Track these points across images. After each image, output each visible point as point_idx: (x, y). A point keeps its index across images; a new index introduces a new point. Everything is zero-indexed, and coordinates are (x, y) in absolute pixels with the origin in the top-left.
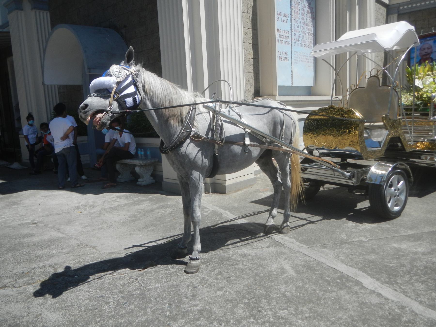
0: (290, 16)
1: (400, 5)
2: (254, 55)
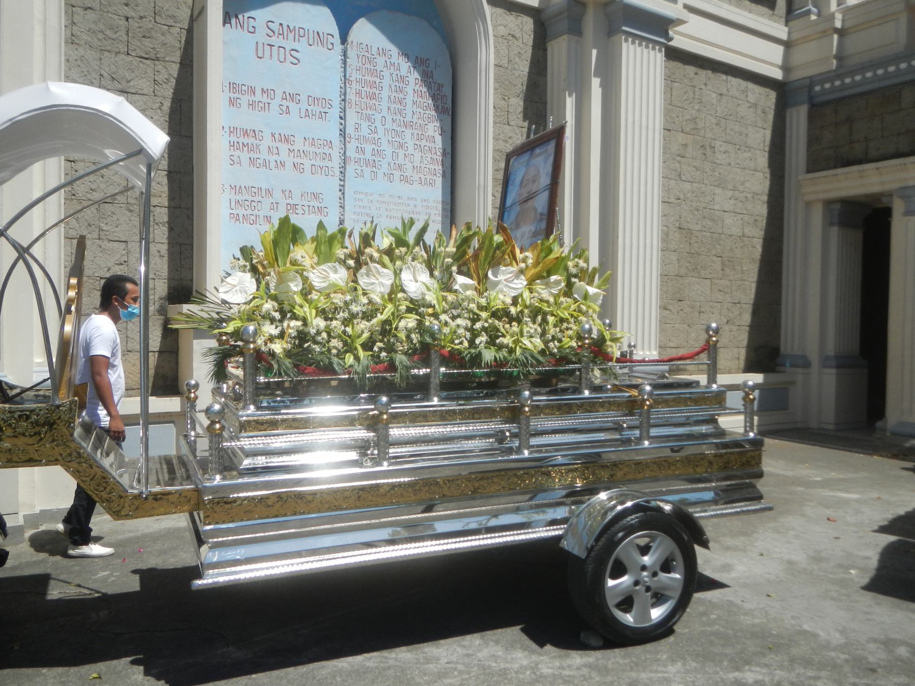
1: (812, 81)
2: (171, 198)
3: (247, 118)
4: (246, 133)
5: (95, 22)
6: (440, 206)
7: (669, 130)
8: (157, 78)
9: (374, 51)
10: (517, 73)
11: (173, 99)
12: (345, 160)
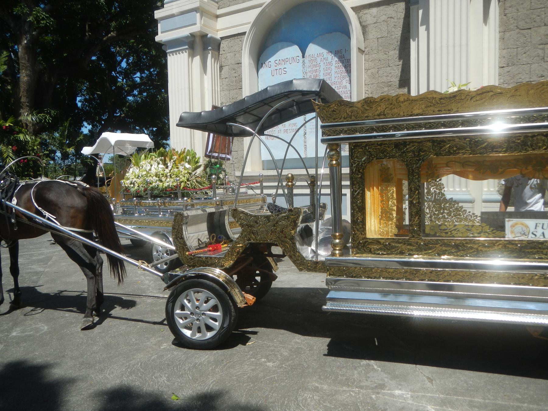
5: (228, 82)
7: (530, 28)
9: (316, 56)
10: (393, 37)
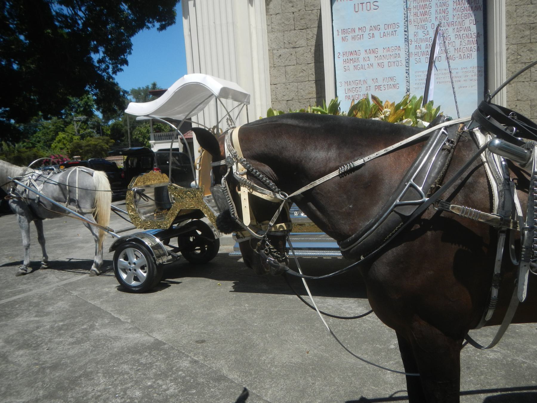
0: (402, 23)
3: (351, 45)
4: (351, 53)
5: (280, 20)
6: (476, 70)
8: (308, 37)
11: (316, 45)
12: (409, 54)
